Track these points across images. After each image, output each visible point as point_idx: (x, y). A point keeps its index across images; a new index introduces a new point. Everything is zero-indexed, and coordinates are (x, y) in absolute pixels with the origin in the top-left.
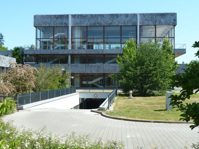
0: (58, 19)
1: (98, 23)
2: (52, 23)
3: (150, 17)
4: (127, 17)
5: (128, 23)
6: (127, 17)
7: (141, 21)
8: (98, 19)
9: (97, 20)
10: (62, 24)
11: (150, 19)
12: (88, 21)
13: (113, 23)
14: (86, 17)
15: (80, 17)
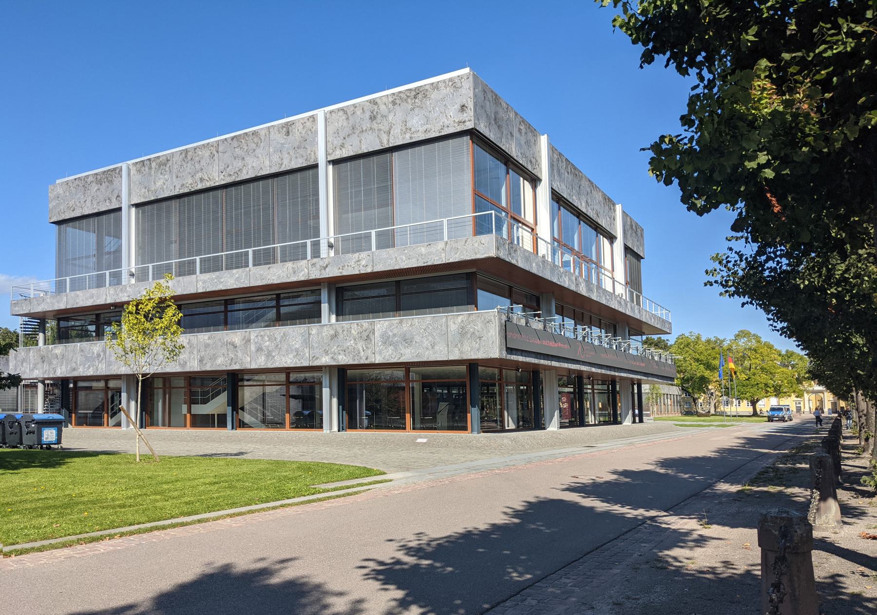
0: (101, 184)
1: (202, 180)
2: (88, 203)
3: (368, 114)
4: (288, 133)
5: (291, 160)
6: (288, 133)
7: (338, 142)
8: (203, 163)
9: (197, 166)
10: (111, 202)
11: (366, 125)
12: (174, 177)
13: (244, 171)
14: (170, 163)
15: (154, 165)
